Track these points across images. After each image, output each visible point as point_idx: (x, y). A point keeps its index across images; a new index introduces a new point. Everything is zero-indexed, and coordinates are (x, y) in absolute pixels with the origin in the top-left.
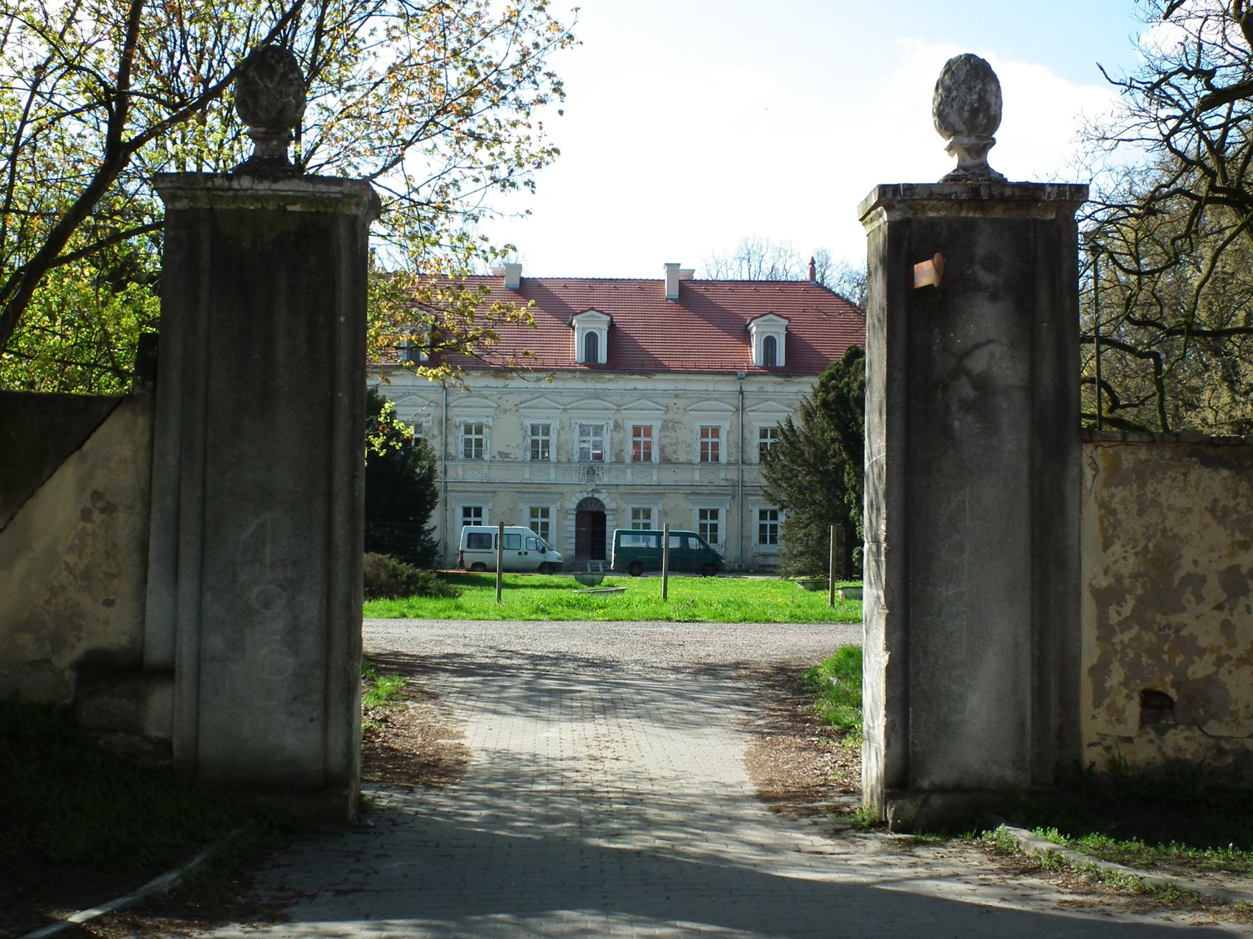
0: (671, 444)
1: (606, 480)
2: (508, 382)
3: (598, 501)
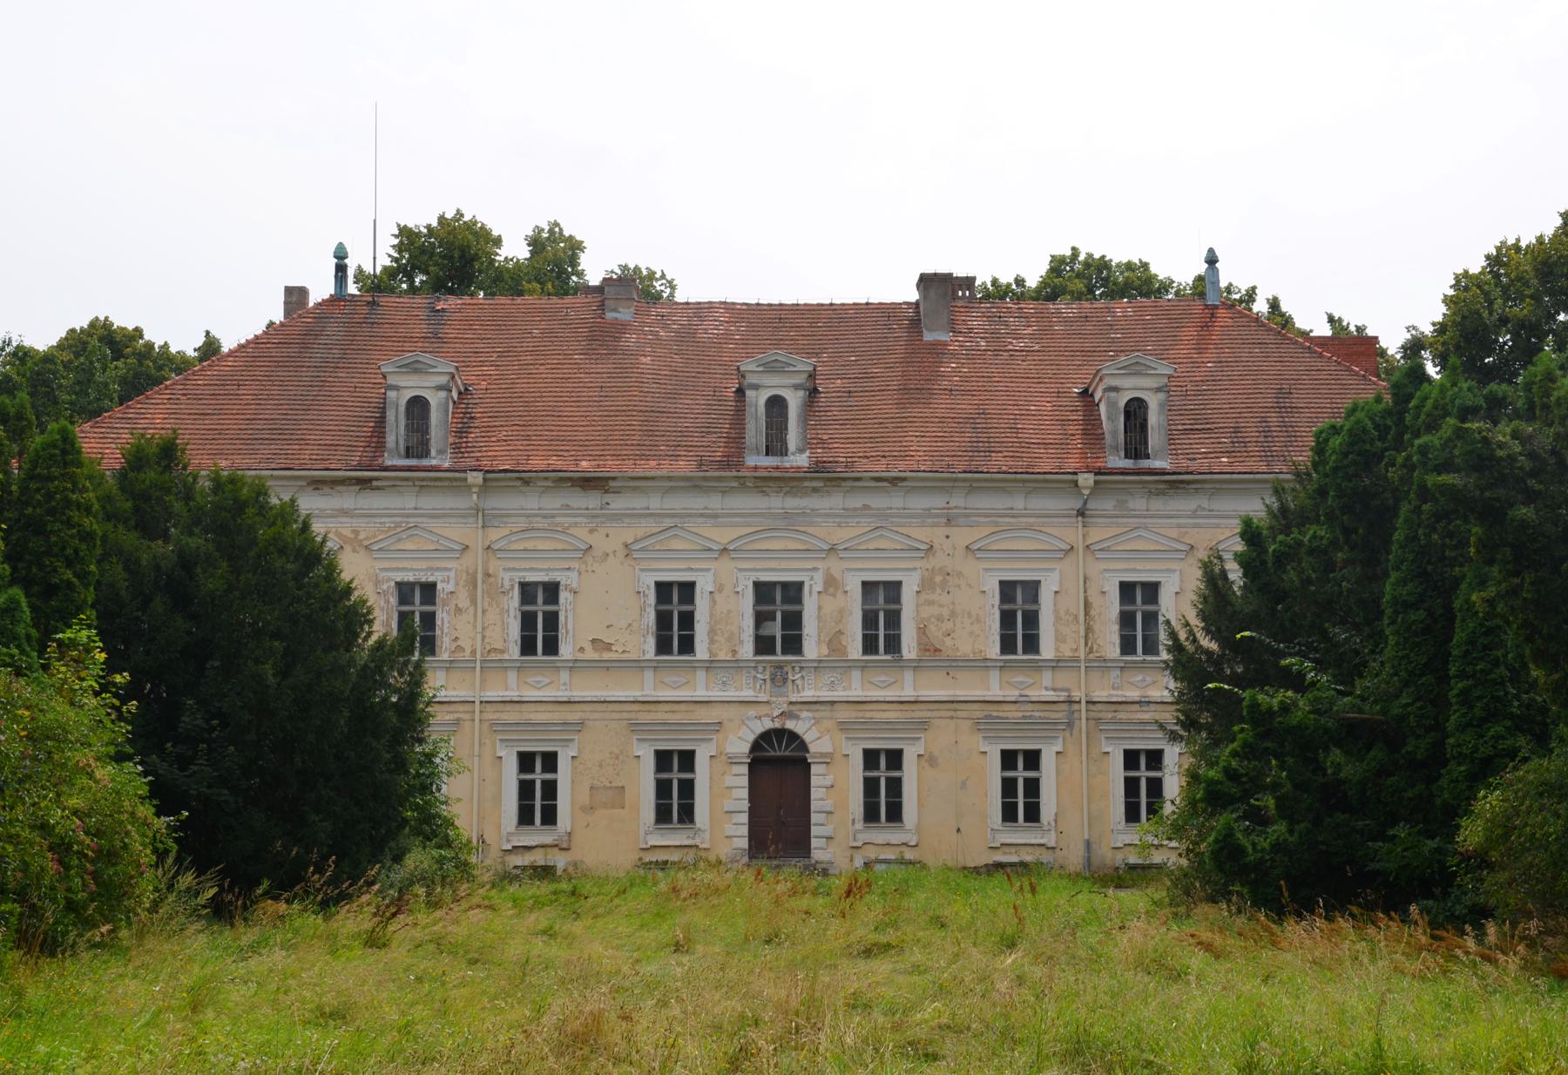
0: (940, 619)
1: (808, 694)
2: (608, 498)
3: (793, 736)
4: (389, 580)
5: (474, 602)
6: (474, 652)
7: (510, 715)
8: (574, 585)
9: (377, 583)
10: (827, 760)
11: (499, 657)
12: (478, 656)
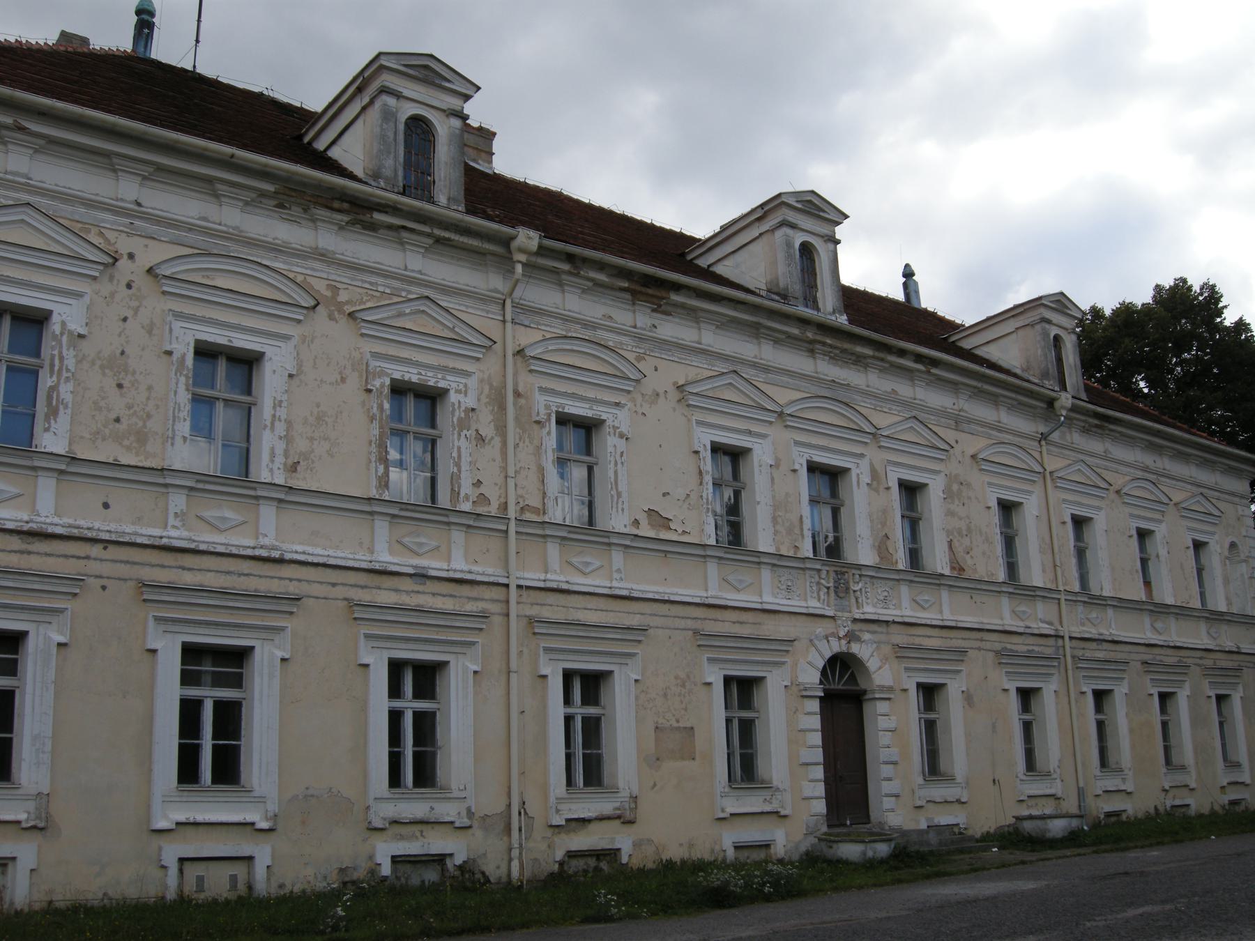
2: (657, 319)
4: (382, 373)
5: (501, 429)
6: (505, 506)
7: (553, 609)
8: (624, 429)
9: (369, 375)
10: (888, 693)
11: (534, 518)
12: (512, 513)
